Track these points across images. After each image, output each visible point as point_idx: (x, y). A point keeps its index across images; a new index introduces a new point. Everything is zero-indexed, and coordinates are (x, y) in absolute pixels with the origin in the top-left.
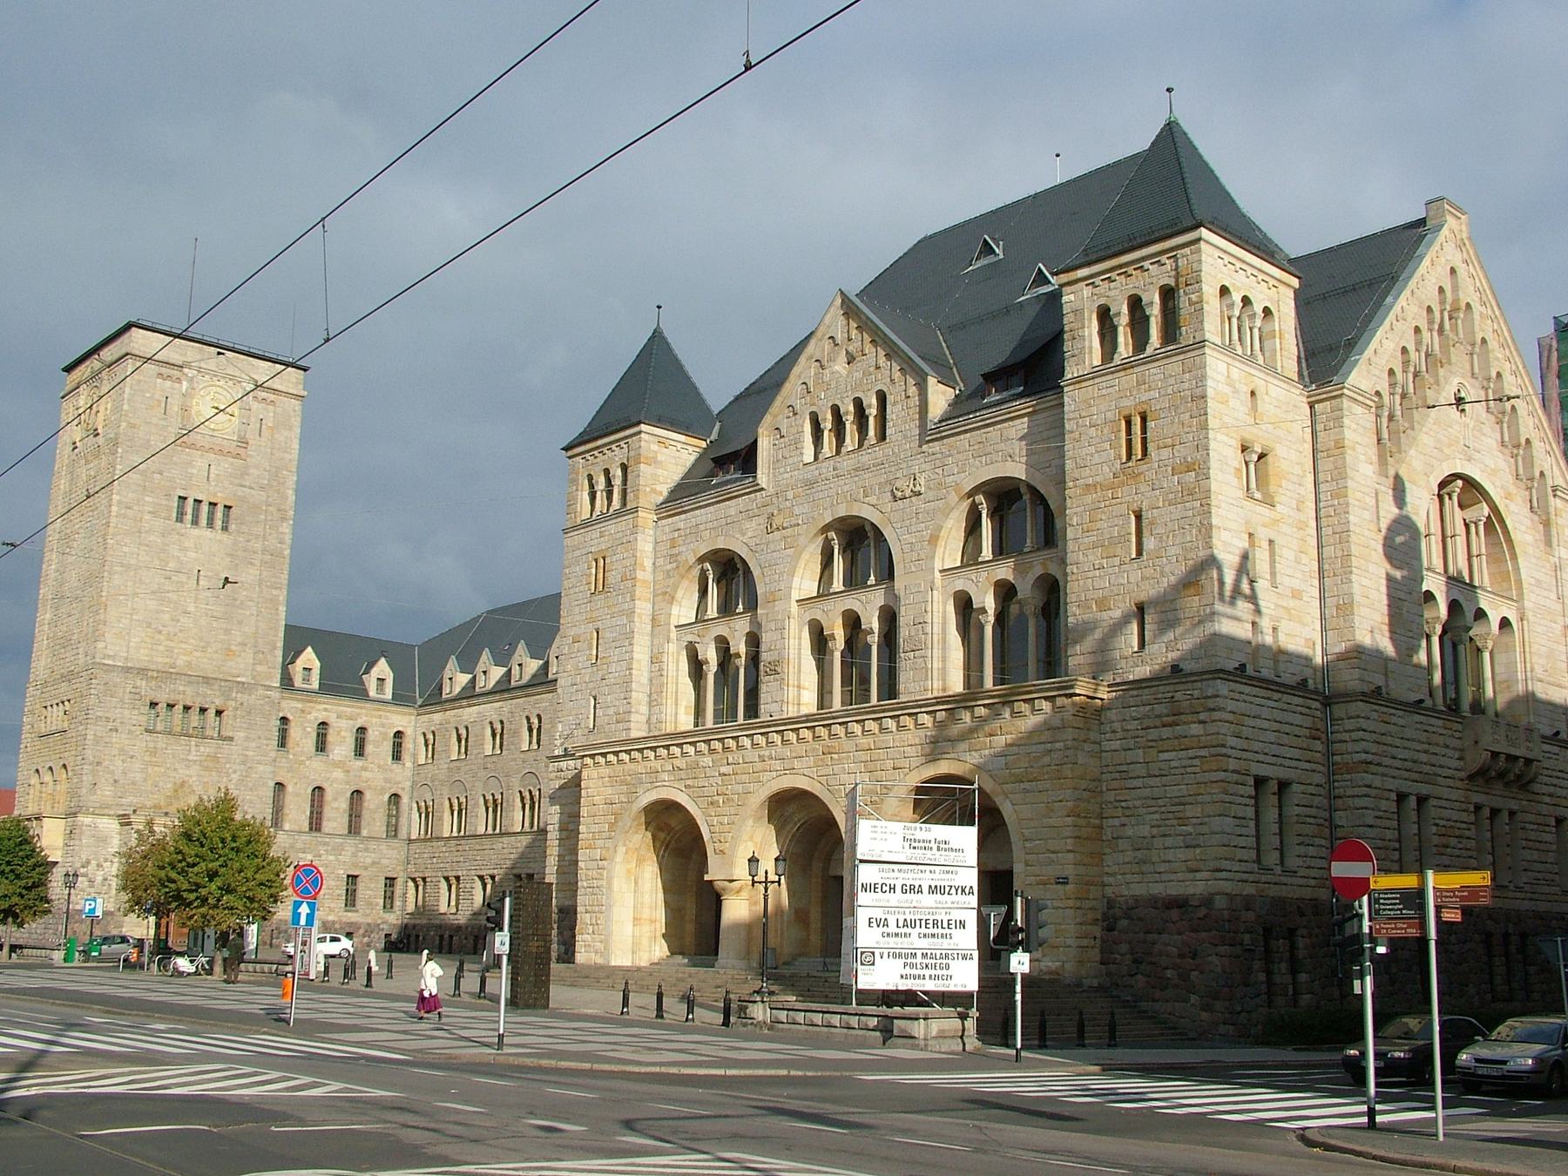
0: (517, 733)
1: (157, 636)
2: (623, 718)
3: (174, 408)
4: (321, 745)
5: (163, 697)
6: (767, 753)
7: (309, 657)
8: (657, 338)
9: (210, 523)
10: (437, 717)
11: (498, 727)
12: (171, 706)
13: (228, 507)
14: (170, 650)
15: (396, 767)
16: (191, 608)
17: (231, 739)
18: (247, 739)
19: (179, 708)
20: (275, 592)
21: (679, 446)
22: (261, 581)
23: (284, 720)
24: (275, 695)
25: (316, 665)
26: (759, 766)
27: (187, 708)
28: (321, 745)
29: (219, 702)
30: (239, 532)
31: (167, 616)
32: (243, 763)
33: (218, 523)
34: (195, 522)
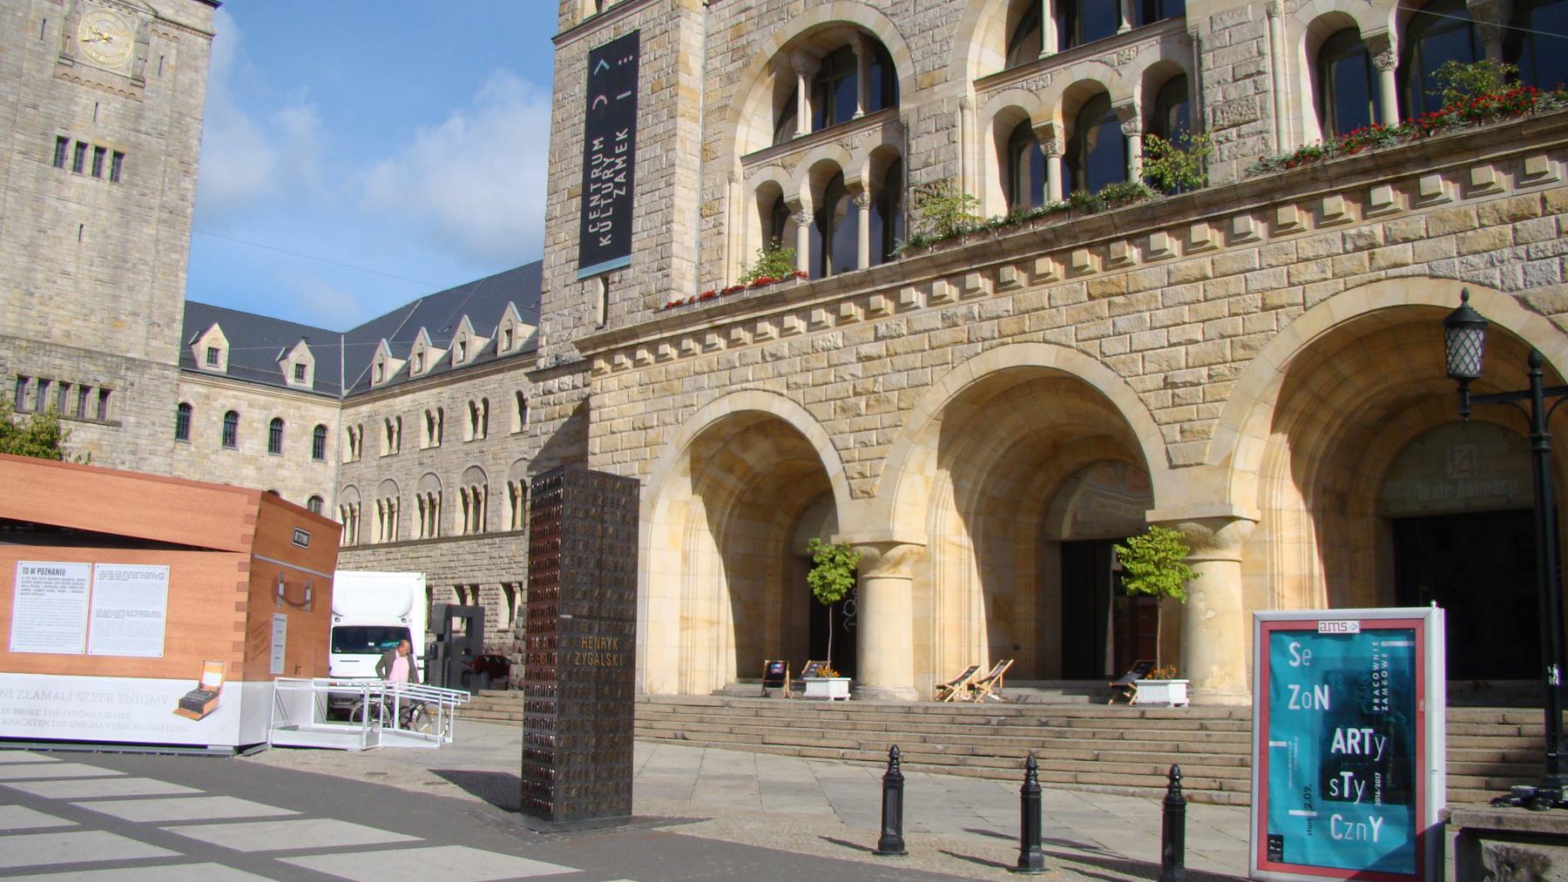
0: (458, 421)
1: (28, 299)
3: (55, 31)
4: (230, 438)
6: (963, 310)
7: (215, 336)
9: (97, 173)
10: (365, 409)
11: (436, 415)
12: (44, 383)
13: (118, 156)
15: (318, 465)
16: (71, 269)
17: (117, 424)
18: (138, 424)
19: (53, 387)
20: (176, 256)
22: (157, 241)
23: (185, 407)
24: (174, 375)
25: (223, 344)
26: (946, 335)
27: (65, 386)
28: (230, 438)
29: (104, 380)
30: (132, 184)
31: (40, 276)
32: (133, 453)
33: (106, 172)
34: (78, 168)
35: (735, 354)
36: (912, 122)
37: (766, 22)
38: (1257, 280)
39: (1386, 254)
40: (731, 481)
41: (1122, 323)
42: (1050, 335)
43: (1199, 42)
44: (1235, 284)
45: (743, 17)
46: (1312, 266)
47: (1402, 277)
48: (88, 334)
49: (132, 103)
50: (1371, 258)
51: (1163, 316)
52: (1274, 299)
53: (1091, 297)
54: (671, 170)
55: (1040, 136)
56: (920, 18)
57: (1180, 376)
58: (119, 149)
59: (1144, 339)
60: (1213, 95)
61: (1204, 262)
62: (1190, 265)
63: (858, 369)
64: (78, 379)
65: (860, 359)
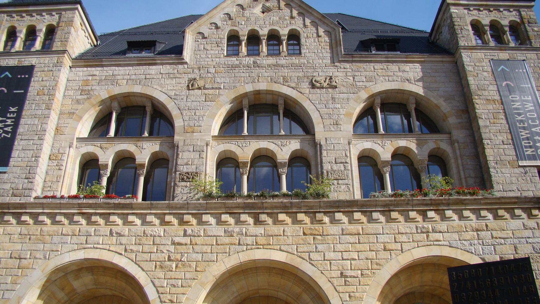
21: (87, 34)
26: (227, 240)
35: (92, 229)
36: (181, 144)
37: (103, 83)
38: (382, 238)
41: (320, 247)
42: (283, 248)
43: (321, 146)
44: (372, 239)
45: (90, 78)
46: (404, 236)
47: (439, 245)
50: (428, 236)
51: (339, 247)
52: (389, 246)
53: (304, 234)
54: (43, 133)
55: (241, 165)
56: (189, 104)
57: (349, 273)
59: (331, 255)
60: (327, 167)
61: (359, 227)
62: (353, 228)
63: (172, 248)
65: (173, 243)
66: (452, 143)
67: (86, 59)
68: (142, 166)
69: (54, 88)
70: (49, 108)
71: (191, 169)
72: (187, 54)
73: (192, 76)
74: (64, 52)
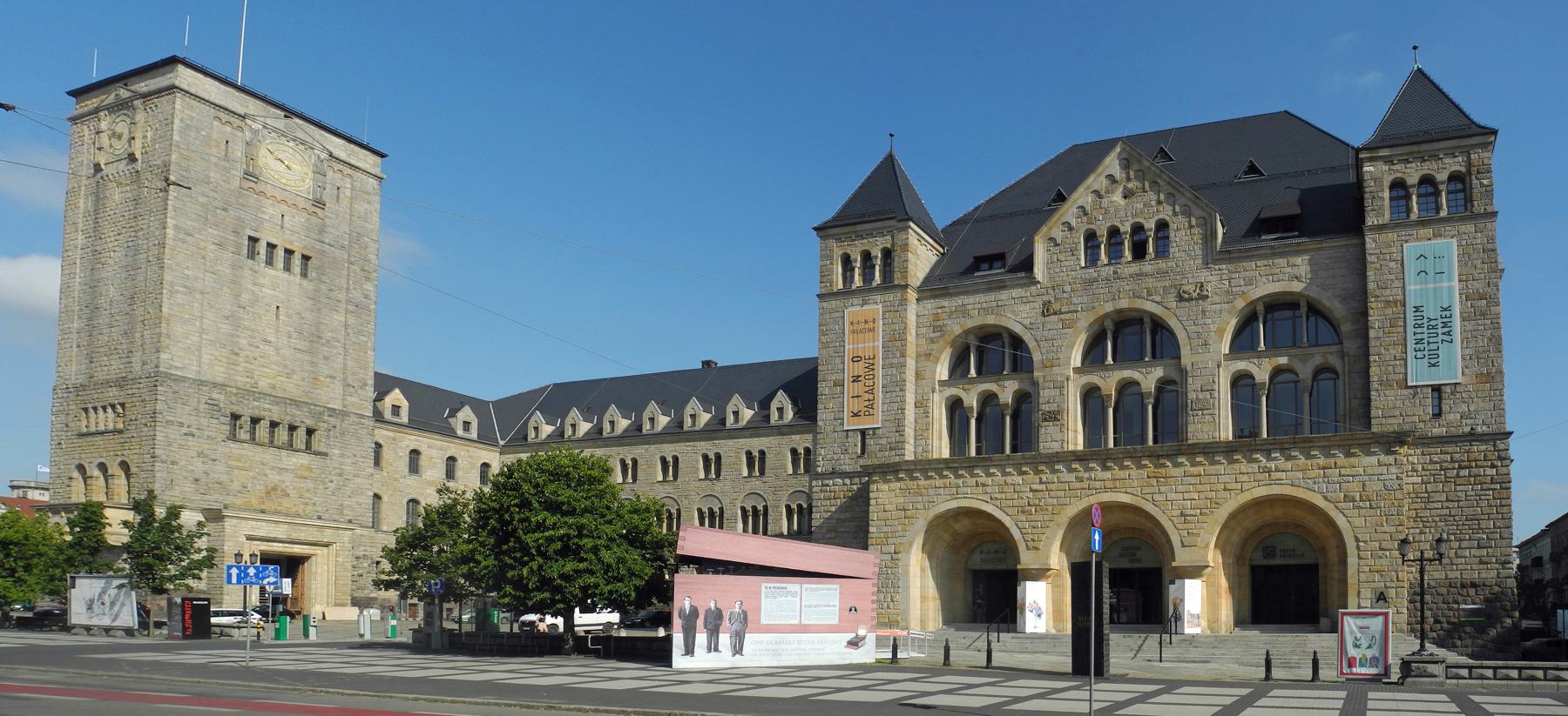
2: (898, 446)
5: (247, 412)
8: (890, 159)
12: (255, 421)
13: (306, 258)
14: (250, 374)
16: (272, 338)
19: (264, 424)
26: (1078, 485)
29: (310, 422)
38: (1222, 478)
39: (1275, 475)
40: (946, 536)
48: (292, 387)
49: (314, 220)
51: (1181, 488)
57: (1189, 512)
58: (307, 253)
59: (1172, 496)
60: (1192, 396)
61: (1201, 469)
62: (1194, 470)
64: (287, 419)
66: (1342, 355)
67: (934, 286)
68: (1006, 405)
69: (905, 330)
70: (903, 355)
71: (1054, 407)
72: (1039, 271)
73: (1045, 298)
74: (906, 286)
